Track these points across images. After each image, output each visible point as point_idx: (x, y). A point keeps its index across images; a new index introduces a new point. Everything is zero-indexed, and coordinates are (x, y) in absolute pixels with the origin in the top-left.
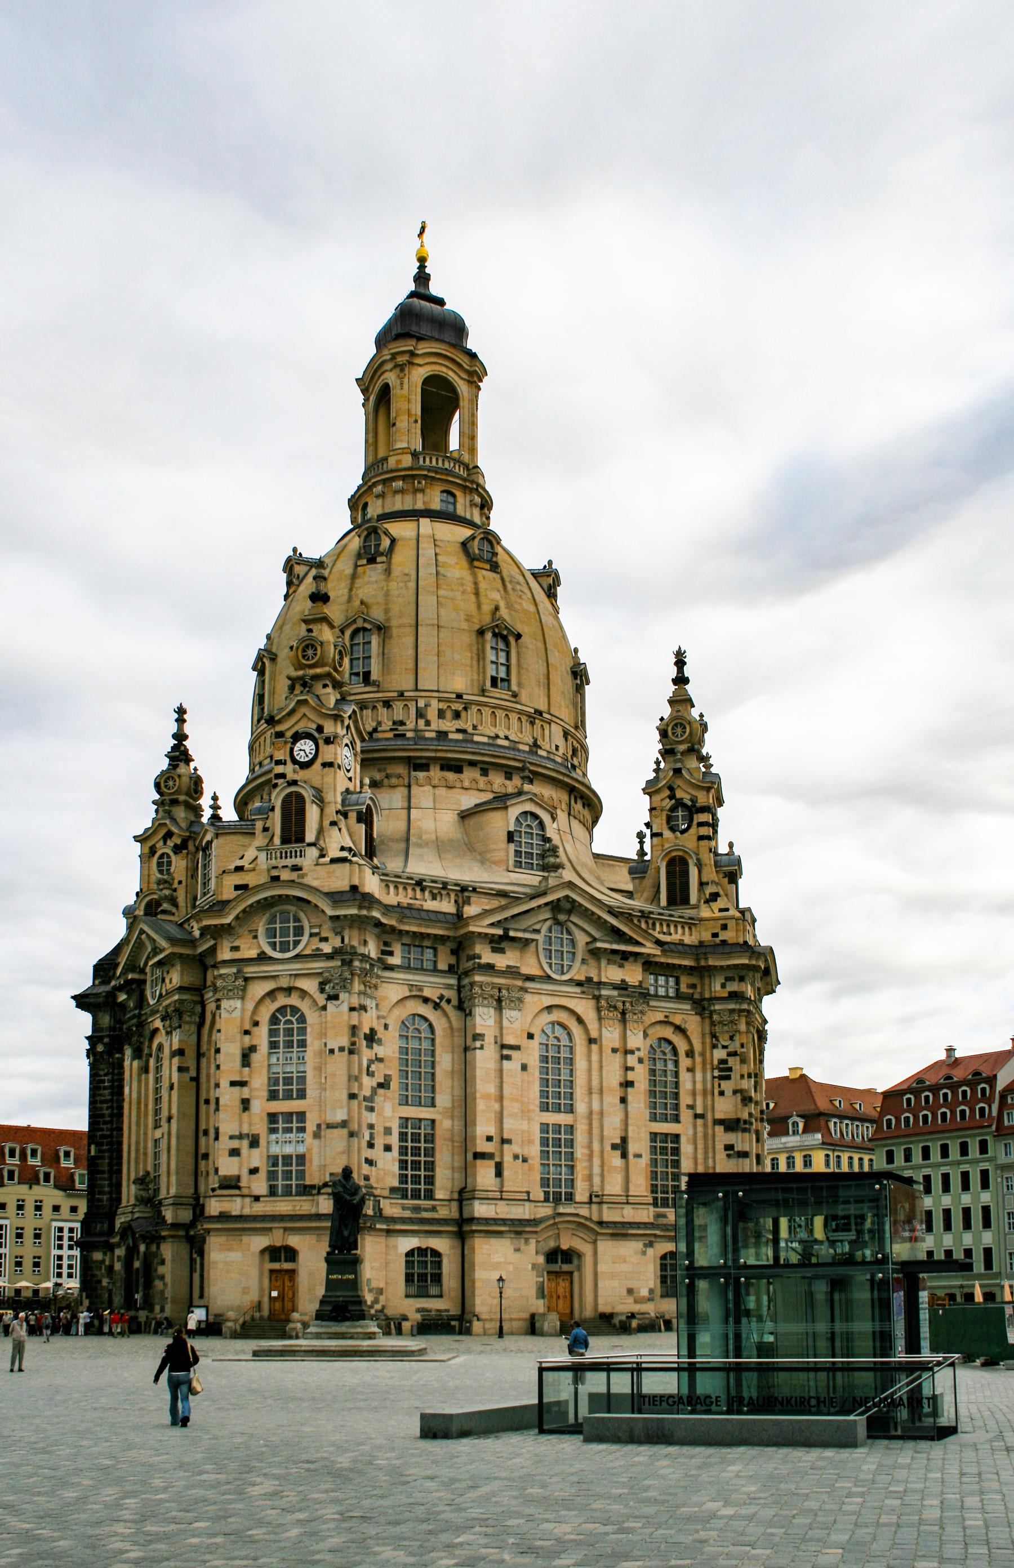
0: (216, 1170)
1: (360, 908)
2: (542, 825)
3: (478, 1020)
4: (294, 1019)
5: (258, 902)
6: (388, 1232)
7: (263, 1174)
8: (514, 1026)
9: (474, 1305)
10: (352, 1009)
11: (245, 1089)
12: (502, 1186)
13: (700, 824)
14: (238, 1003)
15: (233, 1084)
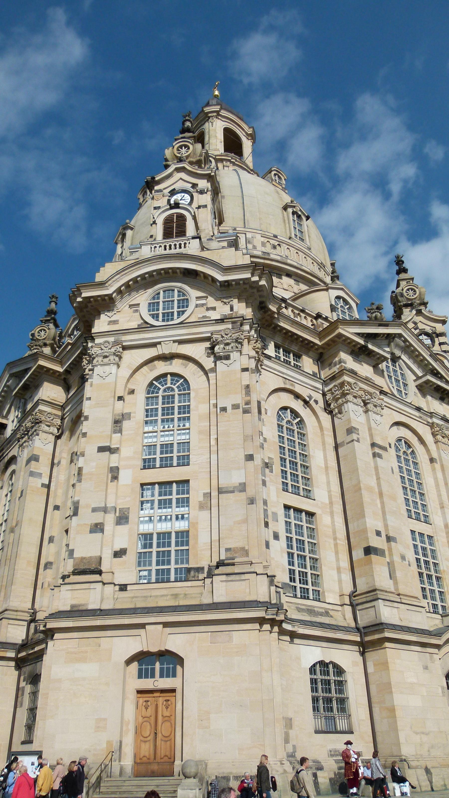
0: (71, 553)
1: (253, 275)
2: (350, 308)
3: (352, 415)
4: (175, 387)
5: (142, 276)
6: (293, 635)
7: (131, 558)
8: (379, 428)
9: (398, 744)
10: (245, 370)
11: (114, 457)
12: (397, 589)
13: (440, 344)
14: (114, 368)
15: (101, 449)
